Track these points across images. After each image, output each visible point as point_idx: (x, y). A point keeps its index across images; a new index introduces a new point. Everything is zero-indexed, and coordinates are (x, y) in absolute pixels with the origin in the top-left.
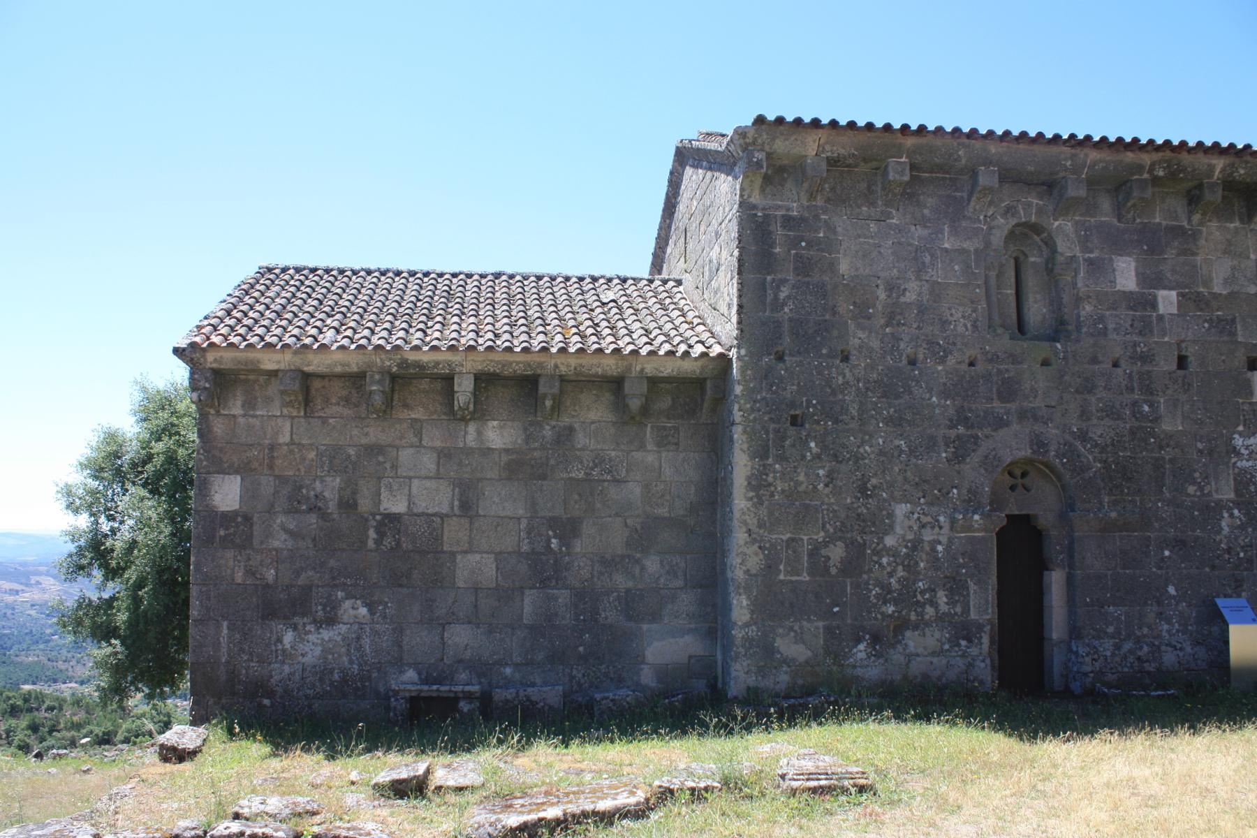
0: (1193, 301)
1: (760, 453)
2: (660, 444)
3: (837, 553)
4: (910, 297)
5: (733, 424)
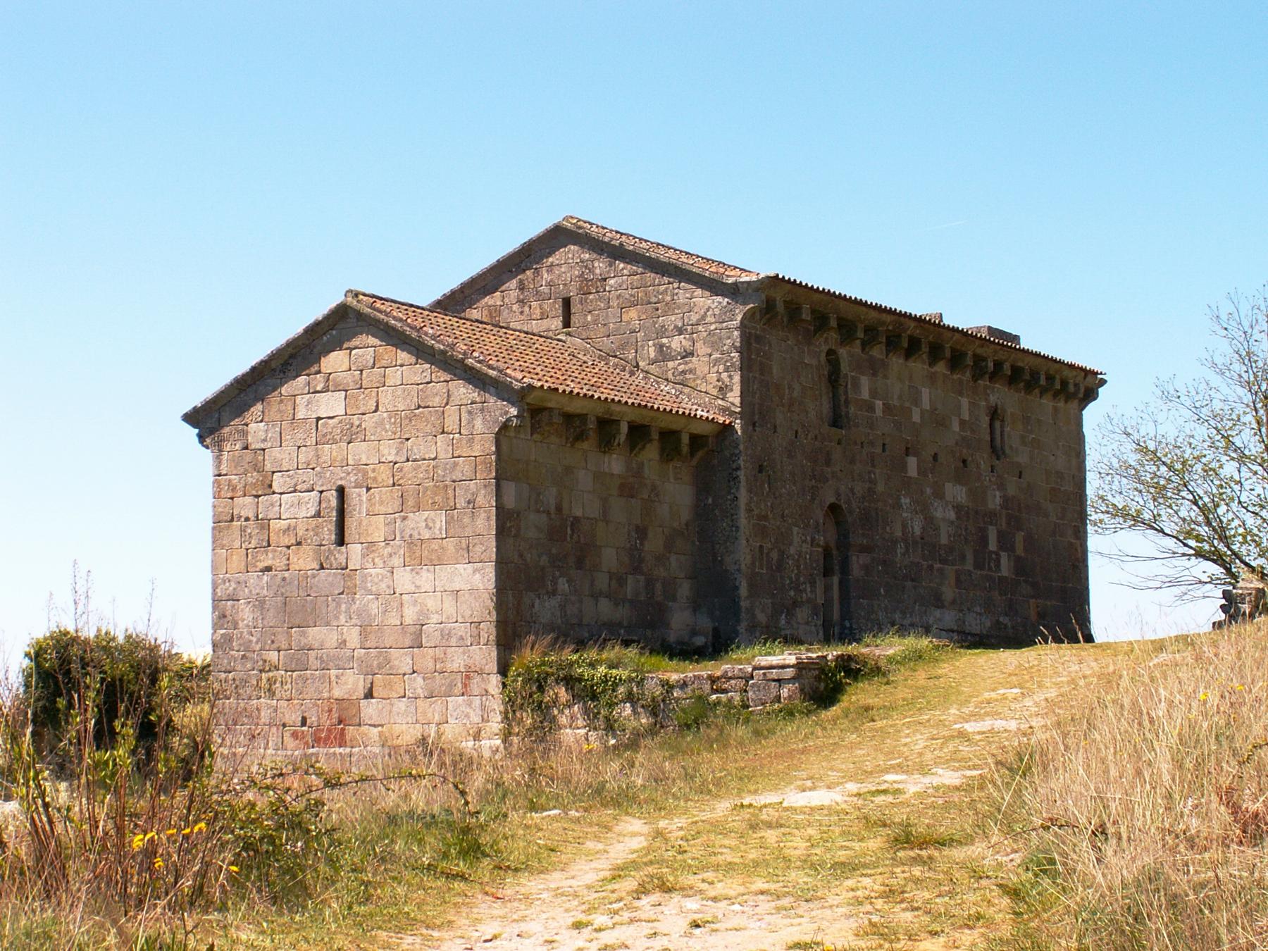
0: (888, 408)
1: (750, 491)
2: (676, 479)
3: (775, 555)
4: (795, 394)
5: (738, 469)
